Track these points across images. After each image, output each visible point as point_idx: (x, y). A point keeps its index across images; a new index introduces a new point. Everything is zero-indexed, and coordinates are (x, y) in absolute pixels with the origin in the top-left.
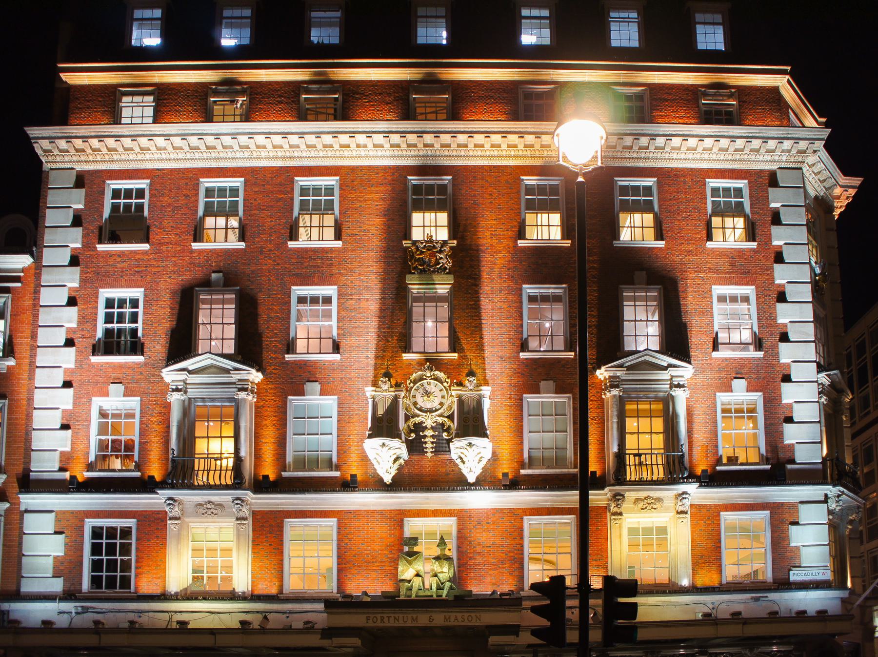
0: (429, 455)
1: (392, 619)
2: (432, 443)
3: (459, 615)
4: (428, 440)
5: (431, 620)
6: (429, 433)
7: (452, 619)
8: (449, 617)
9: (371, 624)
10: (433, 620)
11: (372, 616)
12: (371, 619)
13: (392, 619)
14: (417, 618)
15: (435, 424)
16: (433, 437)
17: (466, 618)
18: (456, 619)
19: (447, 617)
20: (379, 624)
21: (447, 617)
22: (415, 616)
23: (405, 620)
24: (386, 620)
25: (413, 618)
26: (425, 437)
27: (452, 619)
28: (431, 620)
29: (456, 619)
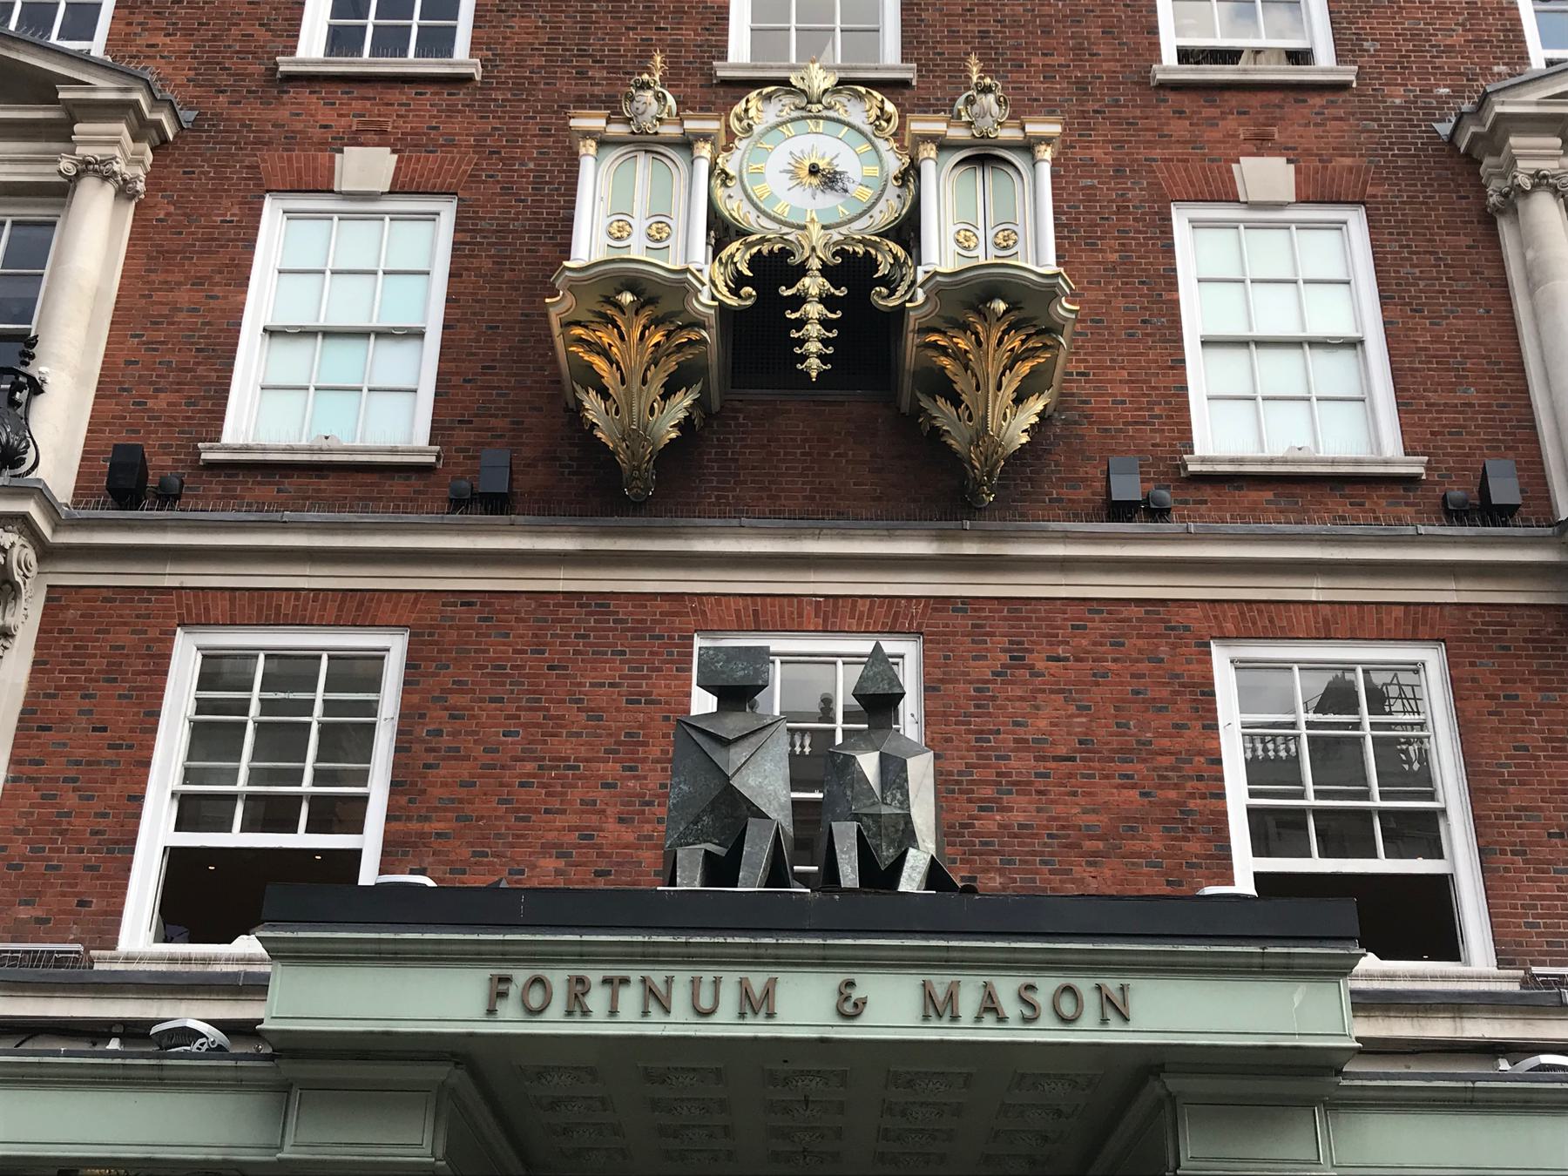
0: (814, 362)
1: (630, 998)
2: (825, 323)
3: (1006, 987)
4: (814, 310)
5: (848, 1008)
6: (813, 284)
7: (969, 1001)
8: (951, 997)
9: (510, 1022)
10: (860, 1005)
11: (521, 976)
12: (514, 990)
13: (630, 998)
14: (768, 993)
15: (839, 260)
16: (827, 301)
17: (1042, 998)
18: (990, 1006)
19: (940, 993)
20: (555, 1024)
21: (940, 993)
22: (758, 980)
23: (705, 1002)
24: (597, 1000)
25: (746, 994)
26: (799, 301)
27: (969, 1001)
28: (849, 1008)
29: (990, 1006)
